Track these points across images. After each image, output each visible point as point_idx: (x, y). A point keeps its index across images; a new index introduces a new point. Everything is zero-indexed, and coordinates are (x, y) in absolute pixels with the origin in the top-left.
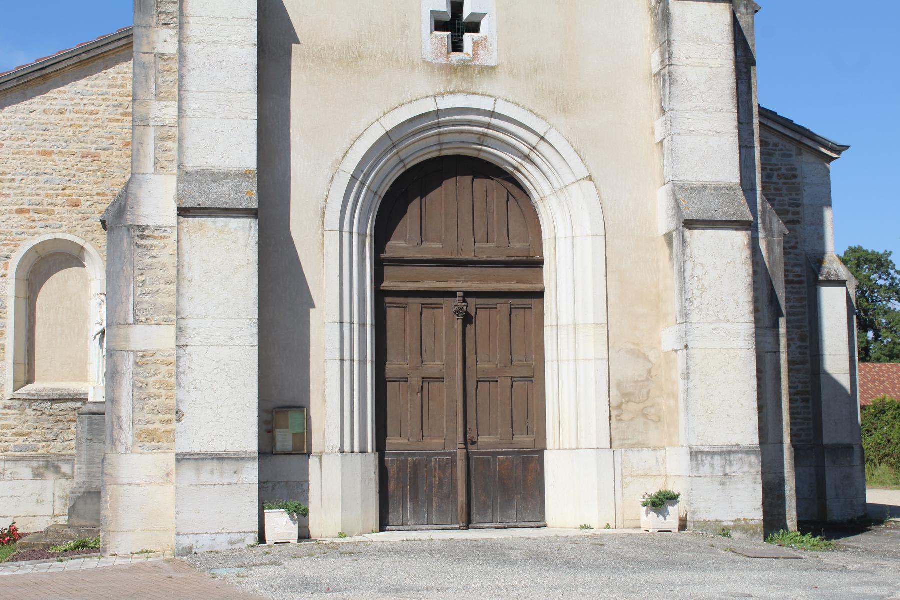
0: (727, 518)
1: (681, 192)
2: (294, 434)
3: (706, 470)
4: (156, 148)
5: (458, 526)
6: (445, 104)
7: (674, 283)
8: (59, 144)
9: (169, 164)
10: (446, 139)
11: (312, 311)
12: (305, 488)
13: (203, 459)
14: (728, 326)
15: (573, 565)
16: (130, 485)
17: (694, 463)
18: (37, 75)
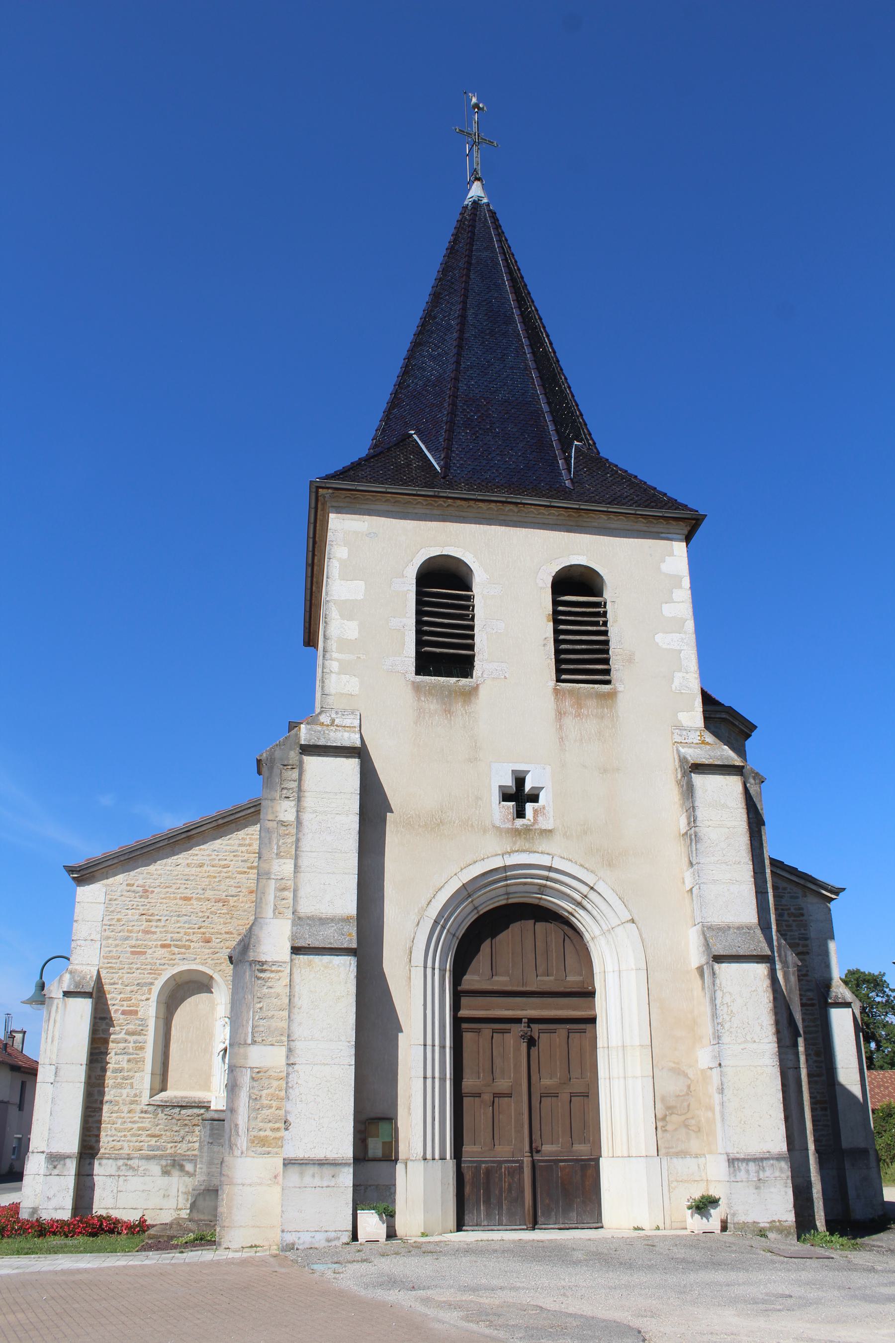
0: (763, 1220)
1: (709, 932)
2: (383, 1143)
3: (742, 1175)
4: (275, 897)
5: (525, 1227)
6: (511, 860)
7: (708, 1010)
8: (196, 891)
9: (285, 910)
11: (400, 1035)
12: (392, 1190)
13: (306, 1164)
14: (755, 1046)
15: (629, 1265)
16: (243, 1185)
17: (732, 1169)
18: (183, 836)
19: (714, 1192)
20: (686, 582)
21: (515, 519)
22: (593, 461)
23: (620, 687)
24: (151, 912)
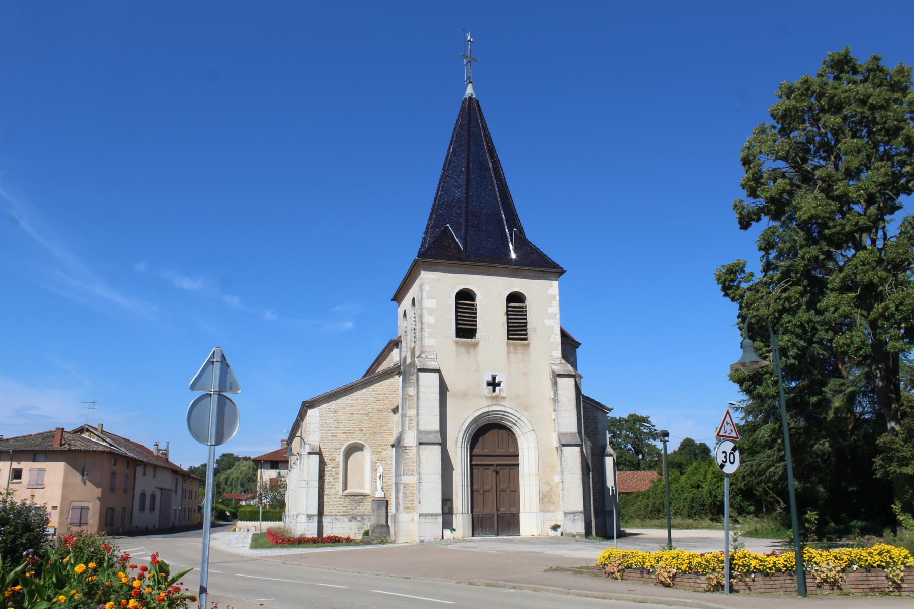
0: (574, 532)
6: (491, 409)
15: (534, 543)
20: (557, 298)
22: (522, 243)
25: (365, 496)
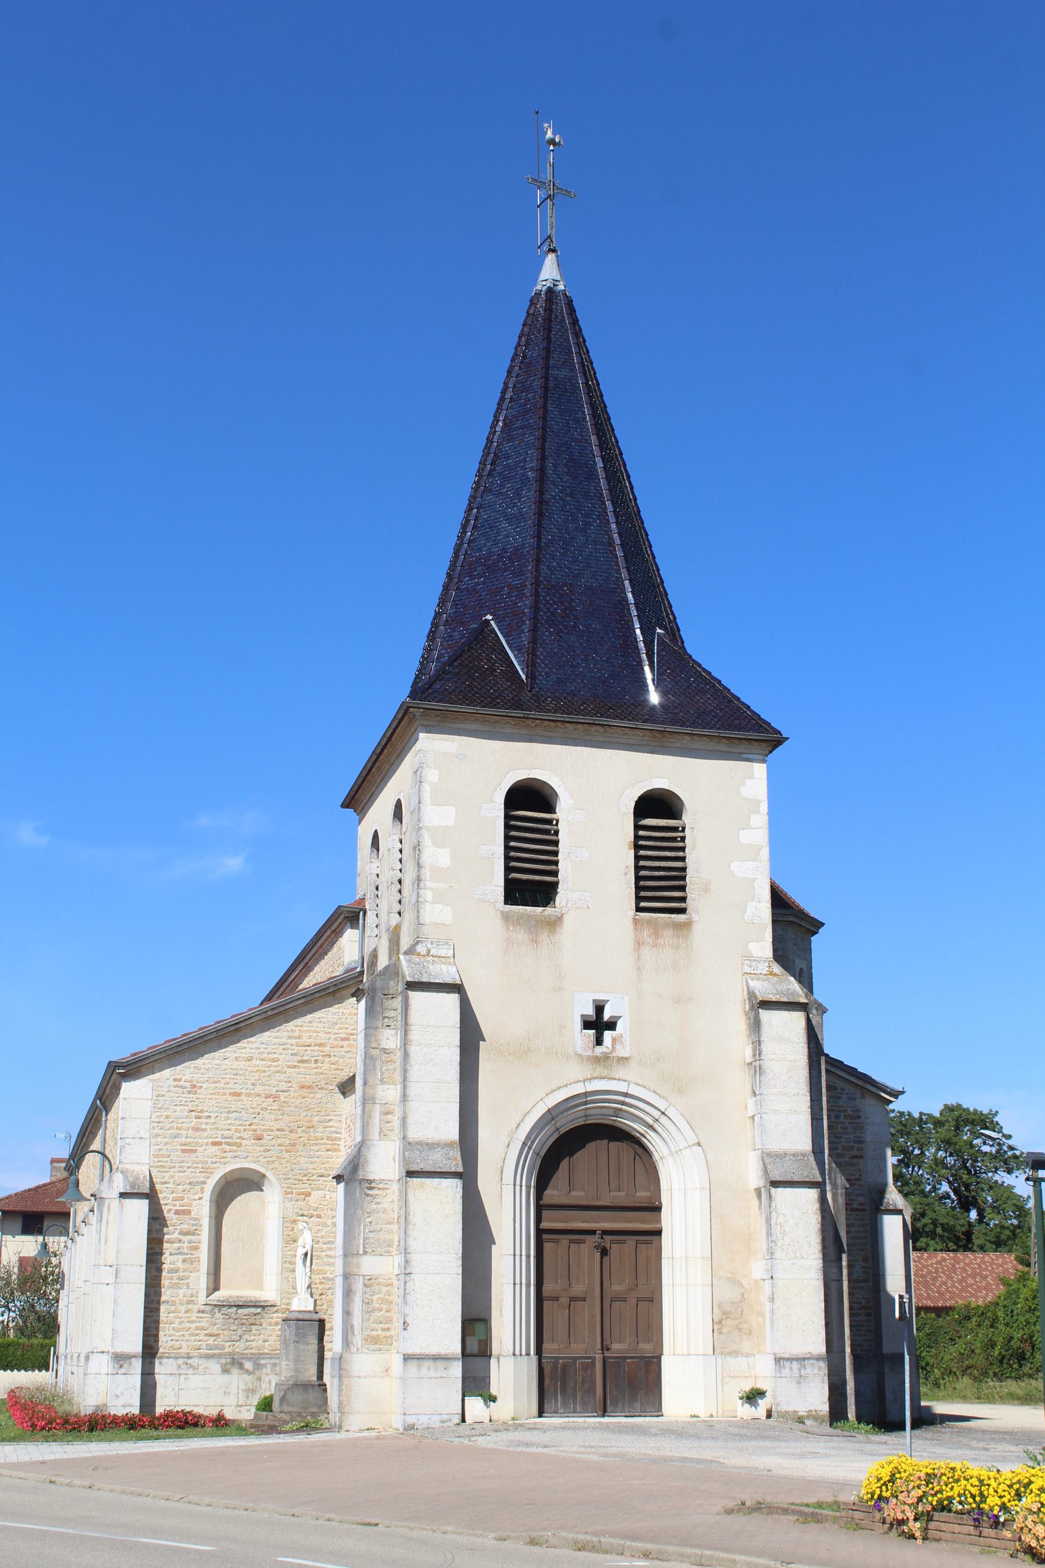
0: (802, 1410)
1: (768, 1158)
3: (786, 1372)
6: (591, 1087)
10: (590, 1112)
15: (697, 1437)
18: (232, 1028)
19: (761, 1385)
20: (764, 807)
21: (600, 739)
22: (677, 665)
23: (695, 917)
24: (200, 1108)
25: (263, 1306)
